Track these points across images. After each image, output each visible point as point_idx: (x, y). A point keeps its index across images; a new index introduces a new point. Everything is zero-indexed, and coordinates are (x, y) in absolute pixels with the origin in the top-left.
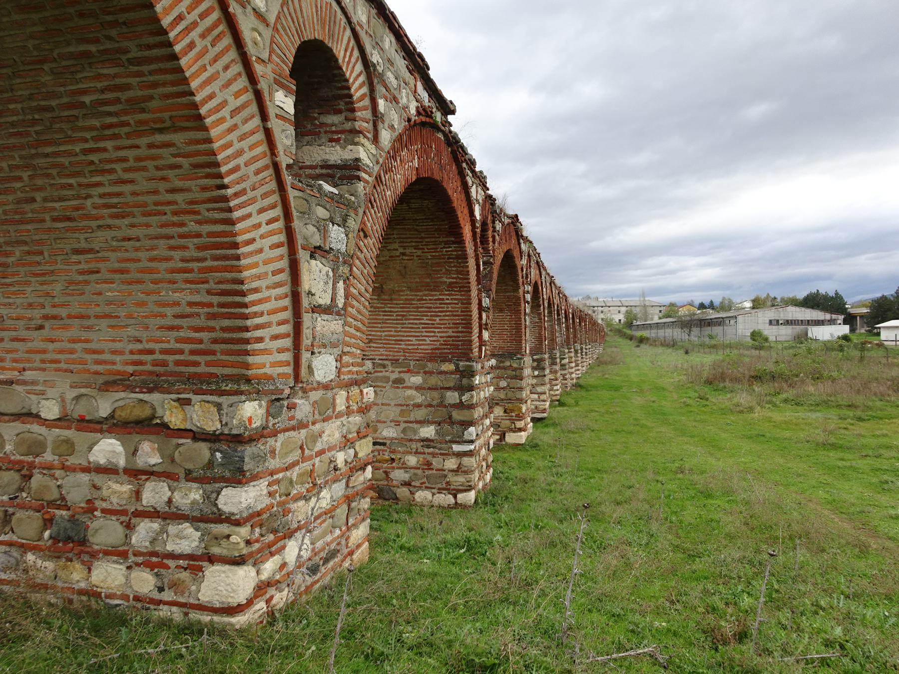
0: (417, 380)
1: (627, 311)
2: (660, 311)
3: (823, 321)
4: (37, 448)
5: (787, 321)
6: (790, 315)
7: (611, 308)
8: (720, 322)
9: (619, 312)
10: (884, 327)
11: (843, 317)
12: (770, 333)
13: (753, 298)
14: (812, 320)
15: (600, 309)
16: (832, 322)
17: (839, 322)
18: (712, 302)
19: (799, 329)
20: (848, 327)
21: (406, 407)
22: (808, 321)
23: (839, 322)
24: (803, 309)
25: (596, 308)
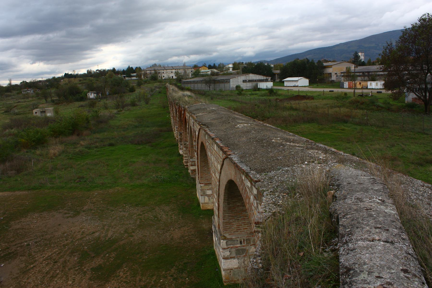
1: (176, 72)
2: (192, 71)
5: (250, 80)
6: (251, 78)
7: (168, 70)
8: (223, 82)
9: (172, 72)
10: (286, 81)
12: (245, 86)
13: (233, 63)
14: (259, 80)
15: (162, 71)
16: (266, 81)
17: (269, 80)
18: (214, 64)
19: (254, 84)
20: (272, 83)
23: (269, 80)
24: (256, 75)
25: (160, 71)
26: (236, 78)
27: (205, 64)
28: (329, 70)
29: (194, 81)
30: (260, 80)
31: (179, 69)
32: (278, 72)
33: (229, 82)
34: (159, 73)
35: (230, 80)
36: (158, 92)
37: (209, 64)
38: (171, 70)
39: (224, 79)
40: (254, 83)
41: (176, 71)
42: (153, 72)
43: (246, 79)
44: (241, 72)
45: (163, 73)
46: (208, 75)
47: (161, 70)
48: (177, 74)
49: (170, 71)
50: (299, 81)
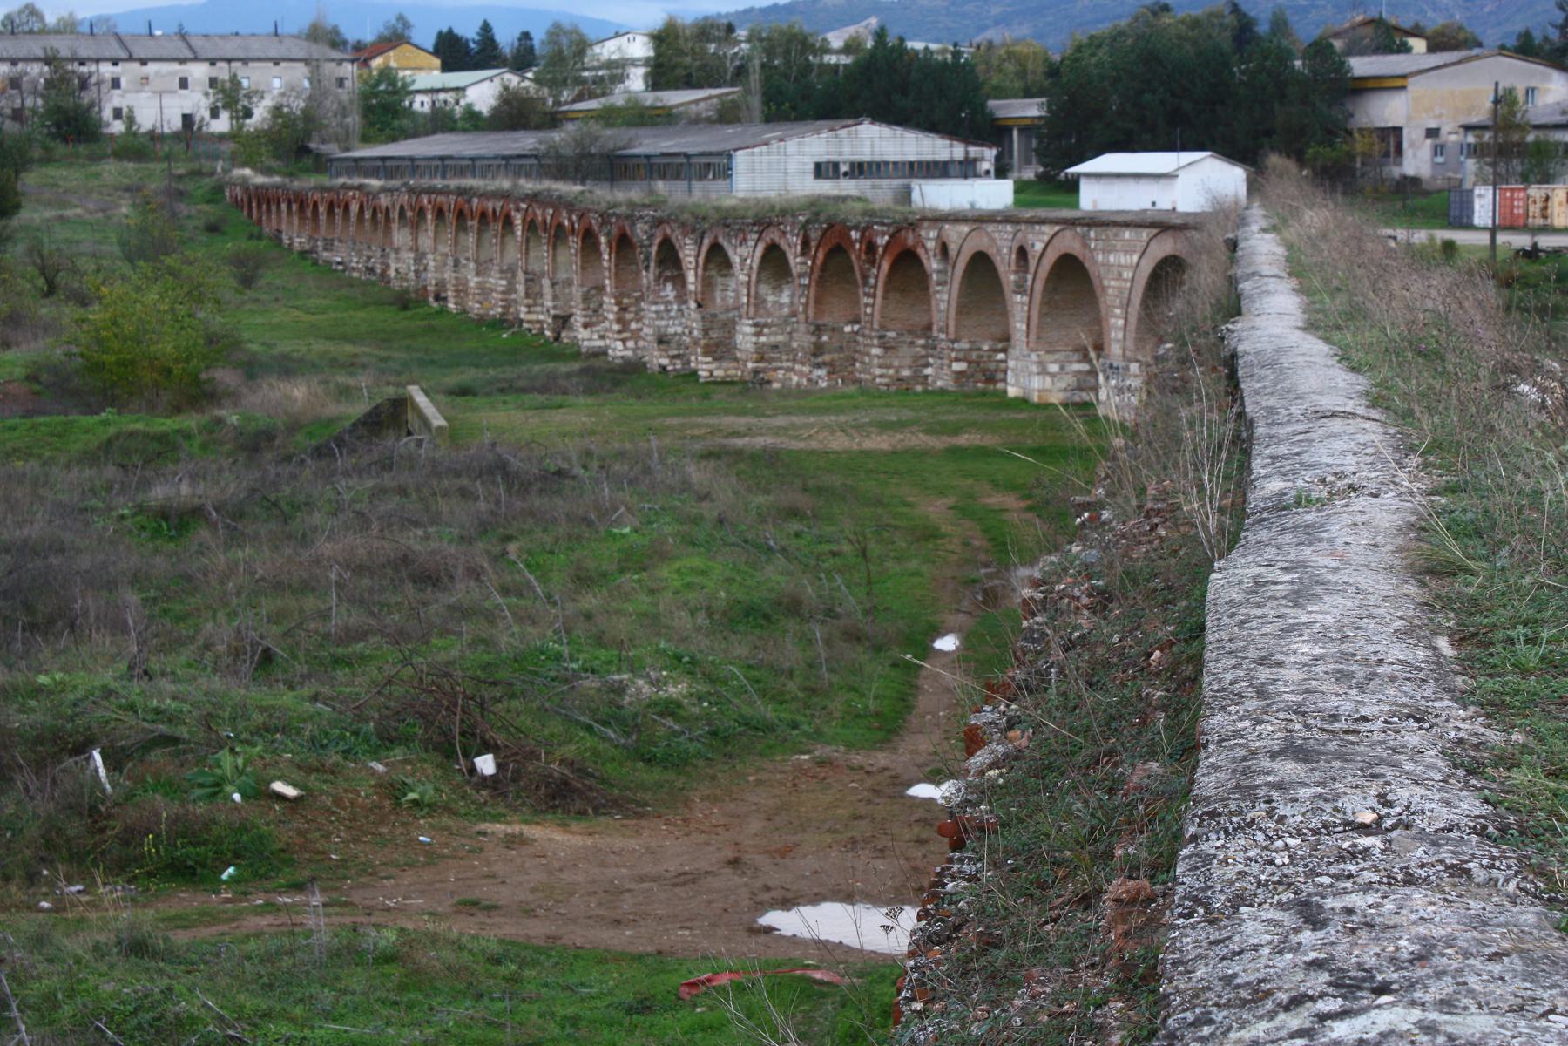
0: (922, 342)
1: (213, 82)
3: (945, 164)
4: (982, 357)
5: (861, 165)
6: (867, 150)
7: (152, 67)
9: (184, 83)
10: (1089, 175)
11: (994, 152)
14: (920, 163)
15: (107, 70)
16: (967, 169)
18: (486, 29)
21: (916, 358)
22: (911, 164)
23: (986, 166)
24: (899, 131)
26: (775, 144)
27: (401, 18)
28: (1388, 110)
29: (442, 158)
30: (928, 164)
31: (245, 61)
32: (1032, 109)
33: (725, 172)
34: (84, 83)
35: (730, 157)
36: (200, 223)
37: (445, 30)
38: (175, 66)
39: (691, 150)
40: (885, 183)
41: (222, 72)
42: (37, 71)
43: (834, 158)
44: (756, 102)
45: (116, 83)
46: (473, 122)
47: (98, 61)
48: (229, 96)
49: (176, 73)
50: (1182, 174)
